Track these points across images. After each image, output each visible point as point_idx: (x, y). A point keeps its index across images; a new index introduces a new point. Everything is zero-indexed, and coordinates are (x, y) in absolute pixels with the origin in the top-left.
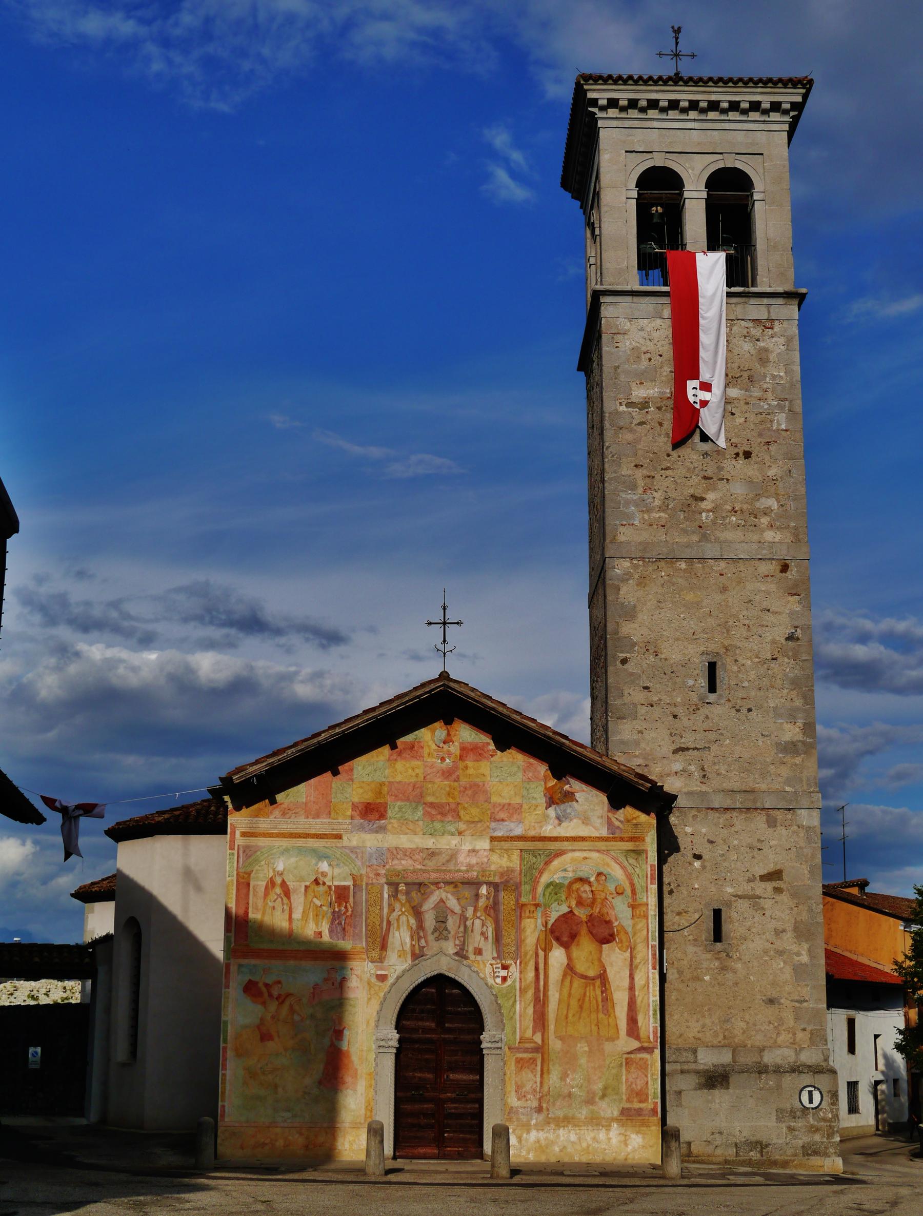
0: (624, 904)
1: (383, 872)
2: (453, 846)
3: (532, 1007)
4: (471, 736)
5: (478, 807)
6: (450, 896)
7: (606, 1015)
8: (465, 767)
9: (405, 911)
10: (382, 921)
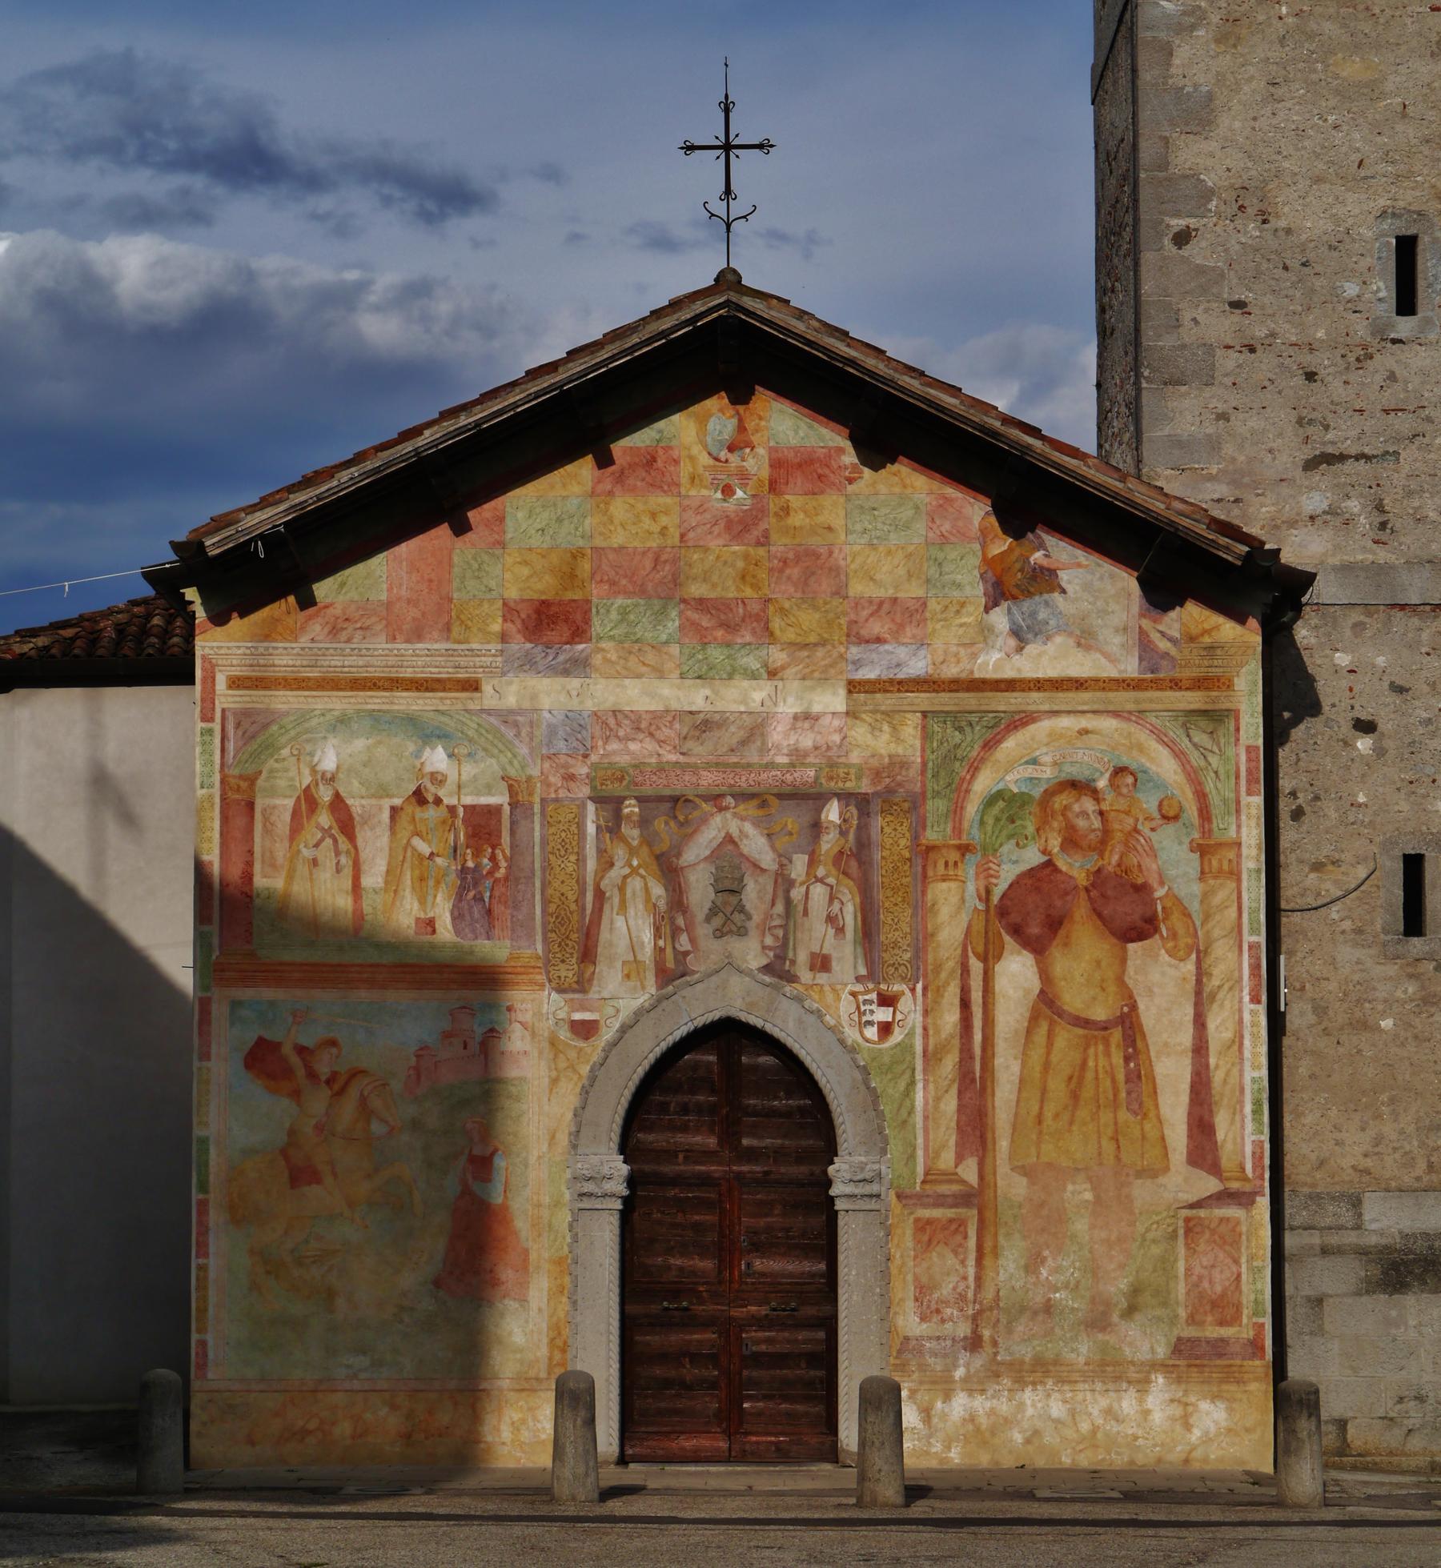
0: (1181, 843)
1: (584, 770)
2: (755, 706)
4: (796, 432)
5: (816, 608)
6: (748, 827)
7: (1136, 1114)
8: (782, 509)
9: (639, 866)
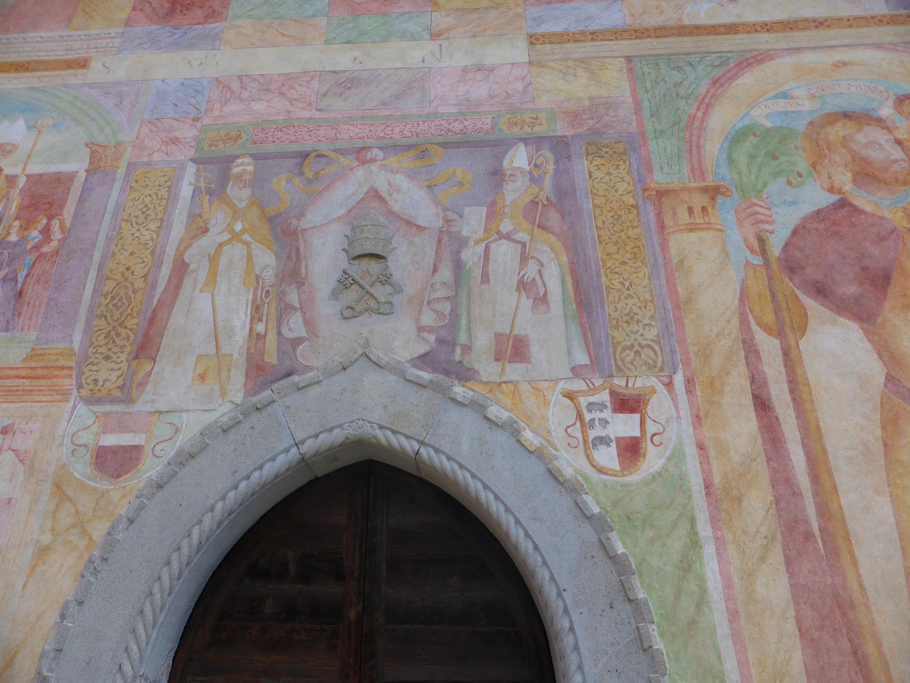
1: (188, 132)
3: (782, 568)
6: (401, 181)
9: (244, 231)
10: (159, 265)
